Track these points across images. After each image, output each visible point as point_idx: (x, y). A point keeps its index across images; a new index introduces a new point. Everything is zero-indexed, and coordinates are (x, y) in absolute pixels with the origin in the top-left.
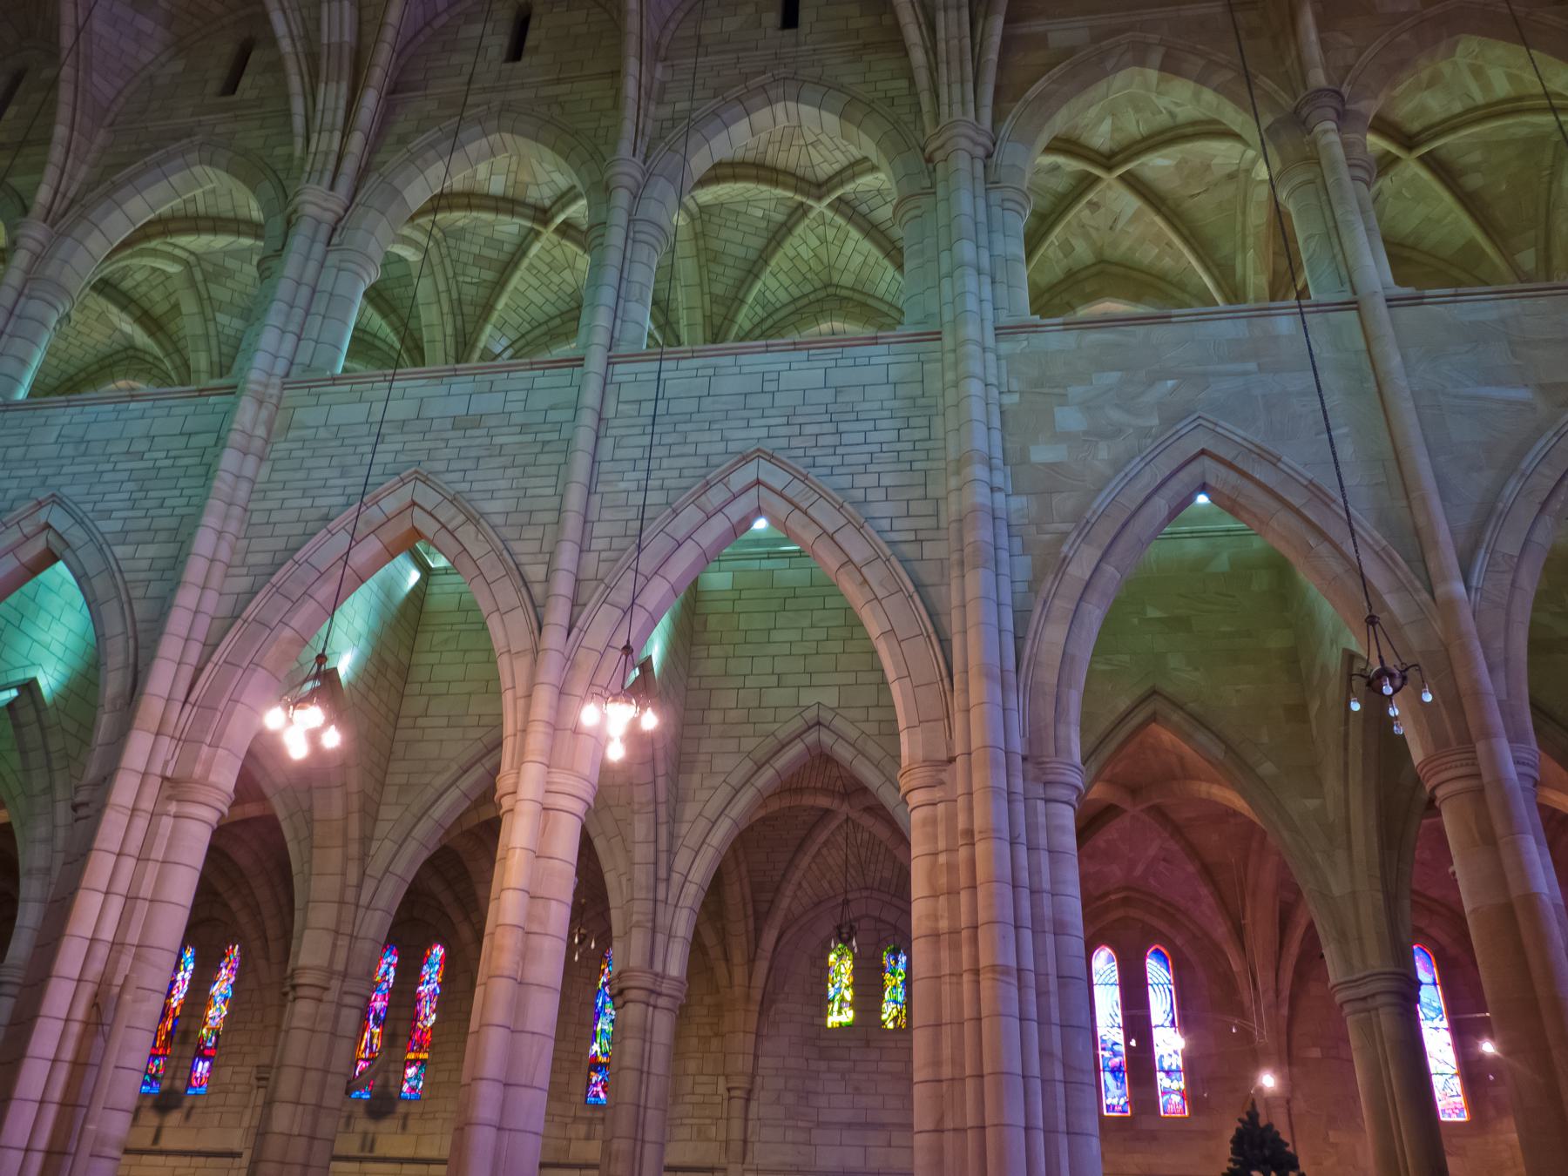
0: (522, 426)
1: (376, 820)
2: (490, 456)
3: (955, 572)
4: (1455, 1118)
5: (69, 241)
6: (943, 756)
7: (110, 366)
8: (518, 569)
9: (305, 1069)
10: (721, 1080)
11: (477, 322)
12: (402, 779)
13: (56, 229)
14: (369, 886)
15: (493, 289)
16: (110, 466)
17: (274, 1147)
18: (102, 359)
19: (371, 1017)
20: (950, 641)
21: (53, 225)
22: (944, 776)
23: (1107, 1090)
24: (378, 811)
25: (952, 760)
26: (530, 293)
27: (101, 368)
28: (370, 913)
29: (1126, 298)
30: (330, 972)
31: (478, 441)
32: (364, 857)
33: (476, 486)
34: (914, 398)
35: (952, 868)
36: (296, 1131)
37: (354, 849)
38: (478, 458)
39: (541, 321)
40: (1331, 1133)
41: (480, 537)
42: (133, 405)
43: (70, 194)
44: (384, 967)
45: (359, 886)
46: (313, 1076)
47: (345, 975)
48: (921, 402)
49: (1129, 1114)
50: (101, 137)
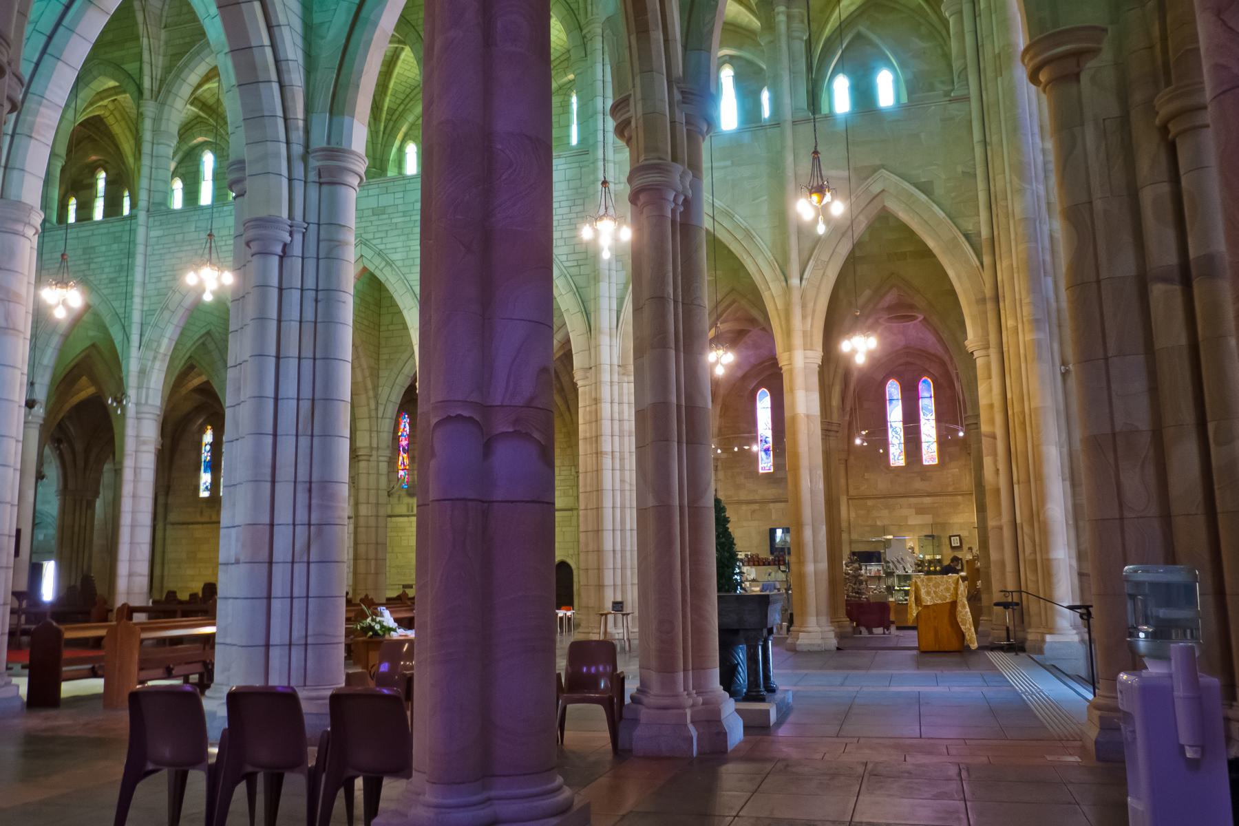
0: (404, 212)
1: (378, 378)
2: (392, 229)
3: (592, 282)
4: (931, 463)
5: (166, 107)
6: (587, 366)
7: (190, 128)
8: (412, 288)
9: (368, 489)
10: (573, 467)
11: (381, 95)
12: (386, 357)
13: (158, 100)
14: (381, 409)
15: (386, 75)
16: (223, 243)
17: (362, 521)
18: (185, 126)
19: (401, 449)
20: (590, 314)
21: (156, 101)
22: (588, 375)
23: (762, 460)
24: (378, 373)
25: (591, 368)
26: (407, 73)
27: (187, 130)
28: (383, 420)
29: (735, 48)
30: (371, 448)
31: (386, 221)
32: (376, 396)
33: (389, 246)
34: (577, 189)
35: (590, 412)
36: (370, 515)
37: (371, 393)
38: (387, 231)
39: (416, 85)
40: (866, 474)
41: (393, 272)
42: (225, 208)
43: (159, 77)
44: (403, 424)
45: (377, 409)
46: (372, 492)
47: (378, 448)
48: (580, 190)
49: (772, 471)
50: (163, 35)
